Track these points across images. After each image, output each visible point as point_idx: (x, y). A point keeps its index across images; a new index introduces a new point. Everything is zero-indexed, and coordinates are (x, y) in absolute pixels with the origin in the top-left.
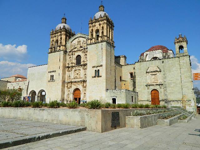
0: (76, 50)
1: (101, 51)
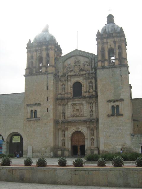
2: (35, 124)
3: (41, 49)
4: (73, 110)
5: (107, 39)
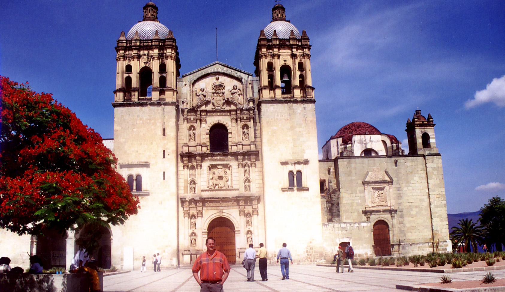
0: (210, 107)
3: (148, 54)
4: (211, 178)
5: (279, 49)
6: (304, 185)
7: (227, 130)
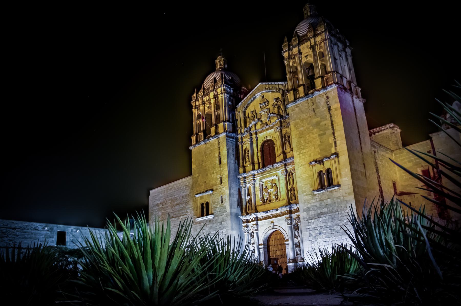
1: (328, 116)
2: (208, 226)
6: (335, 182)
7: (274, 144)
